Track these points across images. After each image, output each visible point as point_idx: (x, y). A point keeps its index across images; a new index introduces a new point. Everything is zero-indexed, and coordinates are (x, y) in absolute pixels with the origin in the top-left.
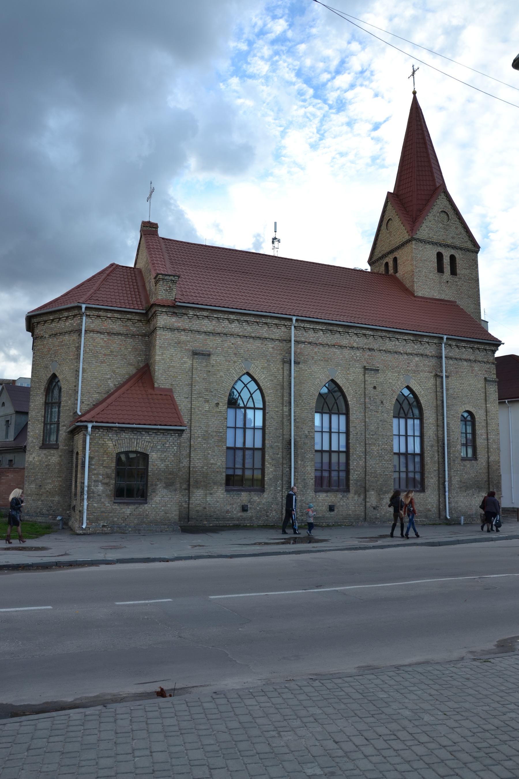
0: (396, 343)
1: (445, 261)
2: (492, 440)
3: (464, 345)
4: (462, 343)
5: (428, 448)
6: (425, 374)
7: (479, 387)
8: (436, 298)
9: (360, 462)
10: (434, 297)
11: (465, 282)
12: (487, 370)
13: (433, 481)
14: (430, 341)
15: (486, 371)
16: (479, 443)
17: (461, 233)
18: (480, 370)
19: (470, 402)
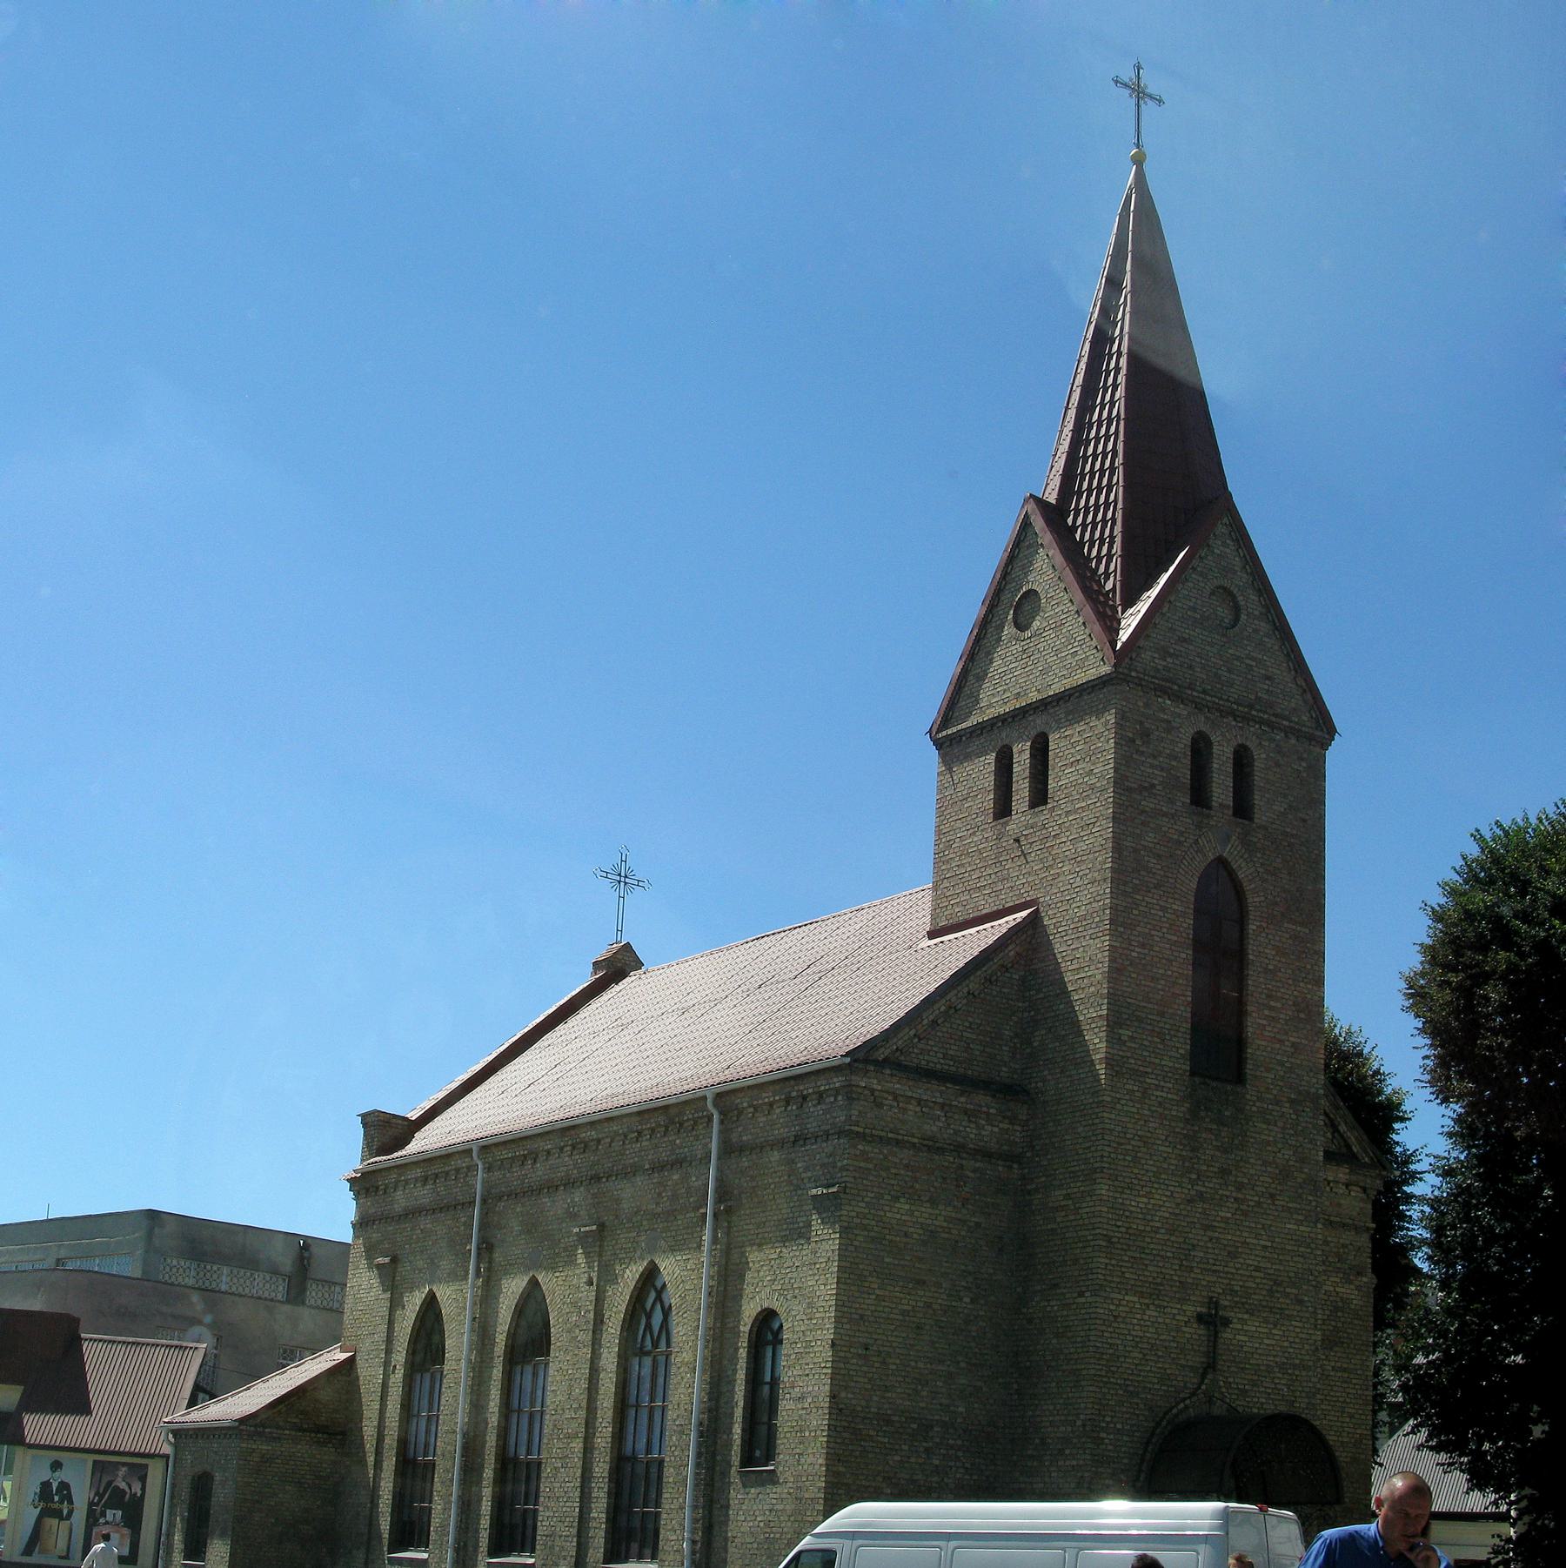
0: (644, 1144)
1: (1016, 768)
2: (809, 1400)
3: (766, 1100)
4: (764, 1095)
5: (674, 1438)
6: (688, 1215)
7: (801, 1225)
8: (984, 912)
9: (555, 1485)
10: (979, 914)
11: (1068, 813)
12: (826, 1160)
13: (674, 1537)
14: (696, 1115)
15: (823, 1165)
16: (784, 1413)
17: (1070, 639)
18: (806, 1169)
19: (775, 1280)
